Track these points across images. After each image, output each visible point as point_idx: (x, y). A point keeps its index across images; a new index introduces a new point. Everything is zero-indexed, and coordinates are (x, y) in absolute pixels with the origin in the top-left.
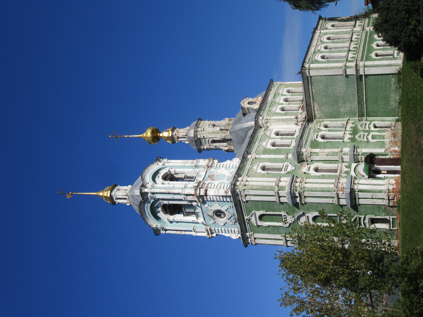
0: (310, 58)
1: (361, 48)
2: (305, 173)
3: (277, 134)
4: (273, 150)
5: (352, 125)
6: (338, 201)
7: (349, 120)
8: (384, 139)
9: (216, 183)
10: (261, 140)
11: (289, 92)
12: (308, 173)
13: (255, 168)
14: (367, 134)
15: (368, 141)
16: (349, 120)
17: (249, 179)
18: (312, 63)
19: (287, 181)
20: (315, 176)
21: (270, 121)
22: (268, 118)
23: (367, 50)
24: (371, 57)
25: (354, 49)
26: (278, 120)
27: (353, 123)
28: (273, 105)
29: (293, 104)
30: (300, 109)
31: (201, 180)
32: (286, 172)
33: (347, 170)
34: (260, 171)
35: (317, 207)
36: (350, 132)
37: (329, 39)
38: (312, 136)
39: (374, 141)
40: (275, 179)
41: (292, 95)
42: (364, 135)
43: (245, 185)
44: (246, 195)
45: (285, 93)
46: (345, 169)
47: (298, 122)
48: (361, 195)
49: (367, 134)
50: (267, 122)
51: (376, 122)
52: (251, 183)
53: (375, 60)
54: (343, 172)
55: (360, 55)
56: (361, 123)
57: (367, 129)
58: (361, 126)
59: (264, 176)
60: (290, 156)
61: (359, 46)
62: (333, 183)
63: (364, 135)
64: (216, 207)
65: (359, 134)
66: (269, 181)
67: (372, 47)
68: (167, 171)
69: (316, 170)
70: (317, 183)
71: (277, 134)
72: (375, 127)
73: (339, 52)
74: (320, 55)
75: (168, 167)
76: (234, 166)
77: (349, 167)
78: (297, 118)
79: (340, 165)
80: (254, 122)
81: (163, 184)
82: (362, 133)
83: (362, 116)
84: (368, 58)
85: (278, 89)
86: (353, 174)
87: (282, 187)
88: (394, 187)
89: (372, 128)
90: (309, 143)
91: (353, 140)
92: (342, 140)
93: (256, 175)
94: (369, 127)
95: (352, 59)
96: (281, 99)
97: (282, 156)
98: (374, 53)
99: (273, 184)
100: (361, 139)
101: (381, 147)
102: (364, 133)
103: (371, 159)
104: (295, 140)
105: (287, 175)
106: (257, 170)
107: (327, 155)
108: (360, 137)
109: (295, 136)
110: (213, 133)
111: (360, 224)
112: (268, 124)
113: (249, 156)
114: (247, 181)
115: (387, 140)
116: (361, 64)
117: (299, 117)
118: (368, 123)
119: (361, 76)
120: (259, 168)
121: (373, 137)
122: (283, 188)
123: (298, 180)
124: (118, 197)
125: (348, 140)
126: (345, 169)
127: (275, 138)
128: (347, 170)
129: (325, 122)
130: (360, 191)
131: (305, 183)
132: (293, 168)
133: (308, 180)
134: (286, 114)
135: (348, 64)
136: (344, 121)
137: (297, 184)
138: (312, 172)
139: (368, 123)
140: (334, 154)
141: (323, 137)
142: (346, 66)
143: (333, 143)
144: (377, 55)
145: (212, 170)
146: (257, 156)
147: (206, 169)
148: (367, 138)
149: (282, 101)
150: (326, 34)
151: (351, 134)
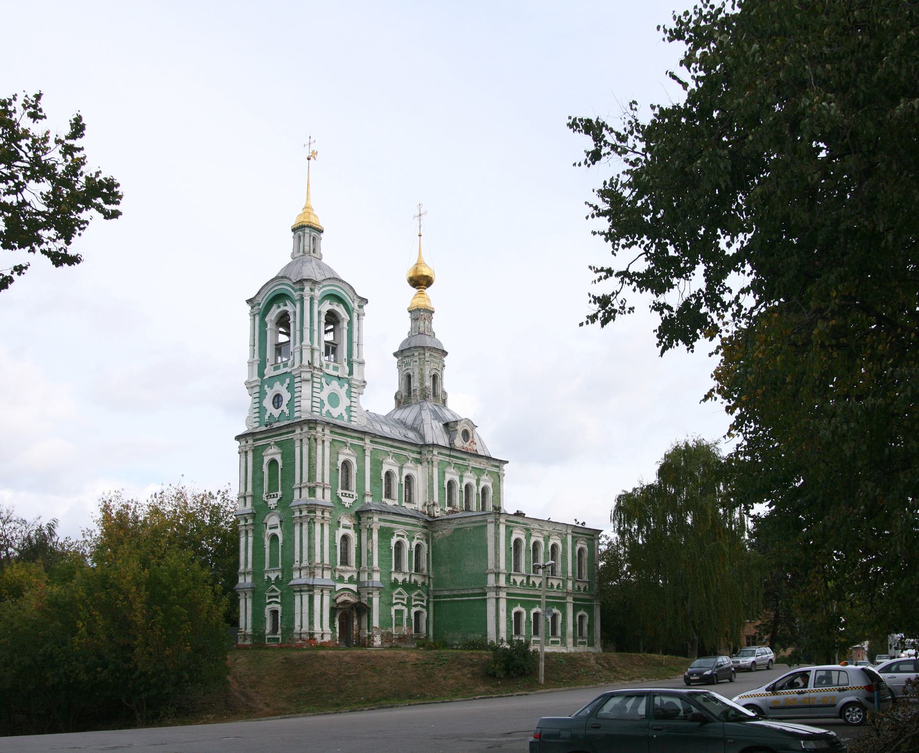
0: (517, 523)
1: (531, 593)
2: (339, 522)
3: (409, 478)
4: (380, 474)
5: (420, 583)
6: (296, 569)
7: (429, 578)
8: (396, 625)
10: (397, 457)
11: (484, 491)
12: (339, 526)
13: (347, 451)
14: (405, 602)
15: (392, 605)
16: (429, 578)
17: (327, 444)
18: (507, 527)
22: (435, 463)
24: (516, 606)
26: (431, 478)
27: (423, 584)
28: (459, 468)
29: (461, 498)
30: (451, 509)
31: (327, 371)
33: (346, 579)
34: (342, 458)
35: (290, 540)
36: (408, 580)
37: (554, 547)
39: (393, 613)
40: (327, 481)
41: (478, 494)
43: (316, 440)
44: (301, 440)
45: (482, 484)
46: (346, 576)
48: (306, 598)
49: (405, 602)
51: (425, 614)
52: (320, 448)
53: (508, 611)
54: (342, 574)
55: (519, 592)
56: (424, 595)
57: (414, 603)
58: (419, 595)
59: (333, 464)
62: (322, 561)
63: (403, 599)
64: (286, 397)
65: (404, 592)
66: (324, 472)
67: (534, 607)
68: (343, 316)
69: (345, 538)
70: (322, 540)
71: (409, 478)
72: (417, 614)
73: (526, 562)
74: (523, 537)
75: (351, 317)
77: (351, 580)
78: (434, 504)
79: (354, 568)
81: (319, 313)
82: (406, 596)
83: (435, 597)
84: (511, 603)
86: (339, 586)
87: (315, 492)
88: (319, 640)
89: (414, 610)
90: (387, 525)
91: (395, 584)
92: (393, 569)
93: (335, 454)
94: (416, 606)
96: (470, 478)
98: (523, 610)
99: (319, 479)
100: (395, 596)
103: (363, 609)
106: (343, 454)
107: (368, 551)
108: (400, 593)
109: (404, 504)
111: (270, 597)
112: (425, 464)
113: (367, 441)
114: (323, 441)
115: (394, 630)
116: (503, 594)
117: (435, 508)
118: (425, 604)
119: (485, 594)
120: (347, 457)
121: (398, 612)
122: (312, 491)
123: (327, 515)
125: (393, 579)
126: (346, 576)
128: (346, 579)
129: (426, 545)
130: (311, 599)
131: (322, 525)
132: (347, 505)
134: (441, 488)
135: (502, 578)
136: (428, 570)
137: (319, 513)
138: (341, 532)
139: (425, 604)
140: (370, 559)
141: (399, 544)
142: (499, 573)
144: (518, 614)
145: (346, 386)
146: (368, 453)
149: (466, 481)
150: (564, 542)
151: (404, 581)
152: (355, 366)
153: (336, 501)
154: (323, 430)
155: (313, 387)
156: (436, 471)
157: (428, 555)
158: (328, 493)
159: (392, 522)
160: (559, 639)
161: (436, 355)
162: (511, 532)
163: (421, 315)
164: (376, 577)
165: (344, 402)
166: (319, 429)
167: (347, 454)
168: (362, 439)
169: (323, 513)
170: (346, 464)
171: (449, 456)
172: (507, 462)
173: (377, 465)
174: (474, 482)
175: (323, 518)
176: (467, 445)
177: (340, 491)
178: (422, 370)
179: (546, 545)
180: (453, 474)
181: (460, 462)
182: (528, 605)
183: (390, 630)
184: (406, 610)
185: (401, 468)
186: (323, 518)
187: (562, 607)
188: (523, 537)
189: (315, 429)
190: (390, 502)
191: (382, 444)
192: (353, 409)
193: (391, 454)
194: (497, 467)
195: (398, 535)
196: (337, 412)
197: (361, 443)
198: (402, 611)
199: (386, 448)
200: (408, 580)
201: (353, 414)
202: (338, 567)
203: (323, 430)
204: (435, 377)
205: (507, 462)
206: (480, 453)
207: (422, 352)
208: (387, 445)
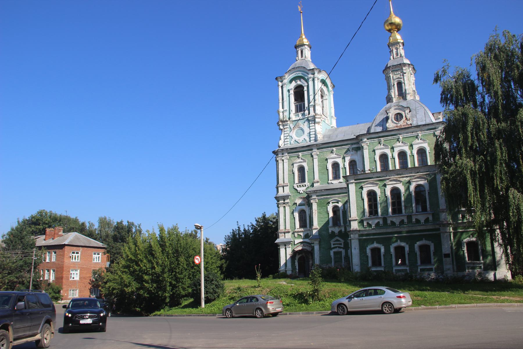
8: (335, 262)
14: (342, 246)
15: (332, 249)
24: (373, 243)
25: (389, 222)
32: (296, 188)
36: (343, 230)
42: (341, 244)
49: (342, 246)
54: (299, 233)
63: (341, 244)
75: (308, 83)
91: (333, 234)
97: (317, 178)
99: (281, 182)
100: (332, 243)
101: (321, 260)
102: (343, 244)
106: (296, 163)
108: (337, 240)
114: (283, 160)
124: (304, 51)
125: (330, 231)
133: (287, 208)
148: (334, 248)
151: (340, 232)
152: (312, 109)
161: (397, 69)
162: (362, 188)
167: (300, 162)
177: (295, 186)
183: (329, 265)
184: (343, 251)
190: (336, 182)
194: (435, 128)
198: (341, 252)
200: (343, 230)
206: (420, 124)
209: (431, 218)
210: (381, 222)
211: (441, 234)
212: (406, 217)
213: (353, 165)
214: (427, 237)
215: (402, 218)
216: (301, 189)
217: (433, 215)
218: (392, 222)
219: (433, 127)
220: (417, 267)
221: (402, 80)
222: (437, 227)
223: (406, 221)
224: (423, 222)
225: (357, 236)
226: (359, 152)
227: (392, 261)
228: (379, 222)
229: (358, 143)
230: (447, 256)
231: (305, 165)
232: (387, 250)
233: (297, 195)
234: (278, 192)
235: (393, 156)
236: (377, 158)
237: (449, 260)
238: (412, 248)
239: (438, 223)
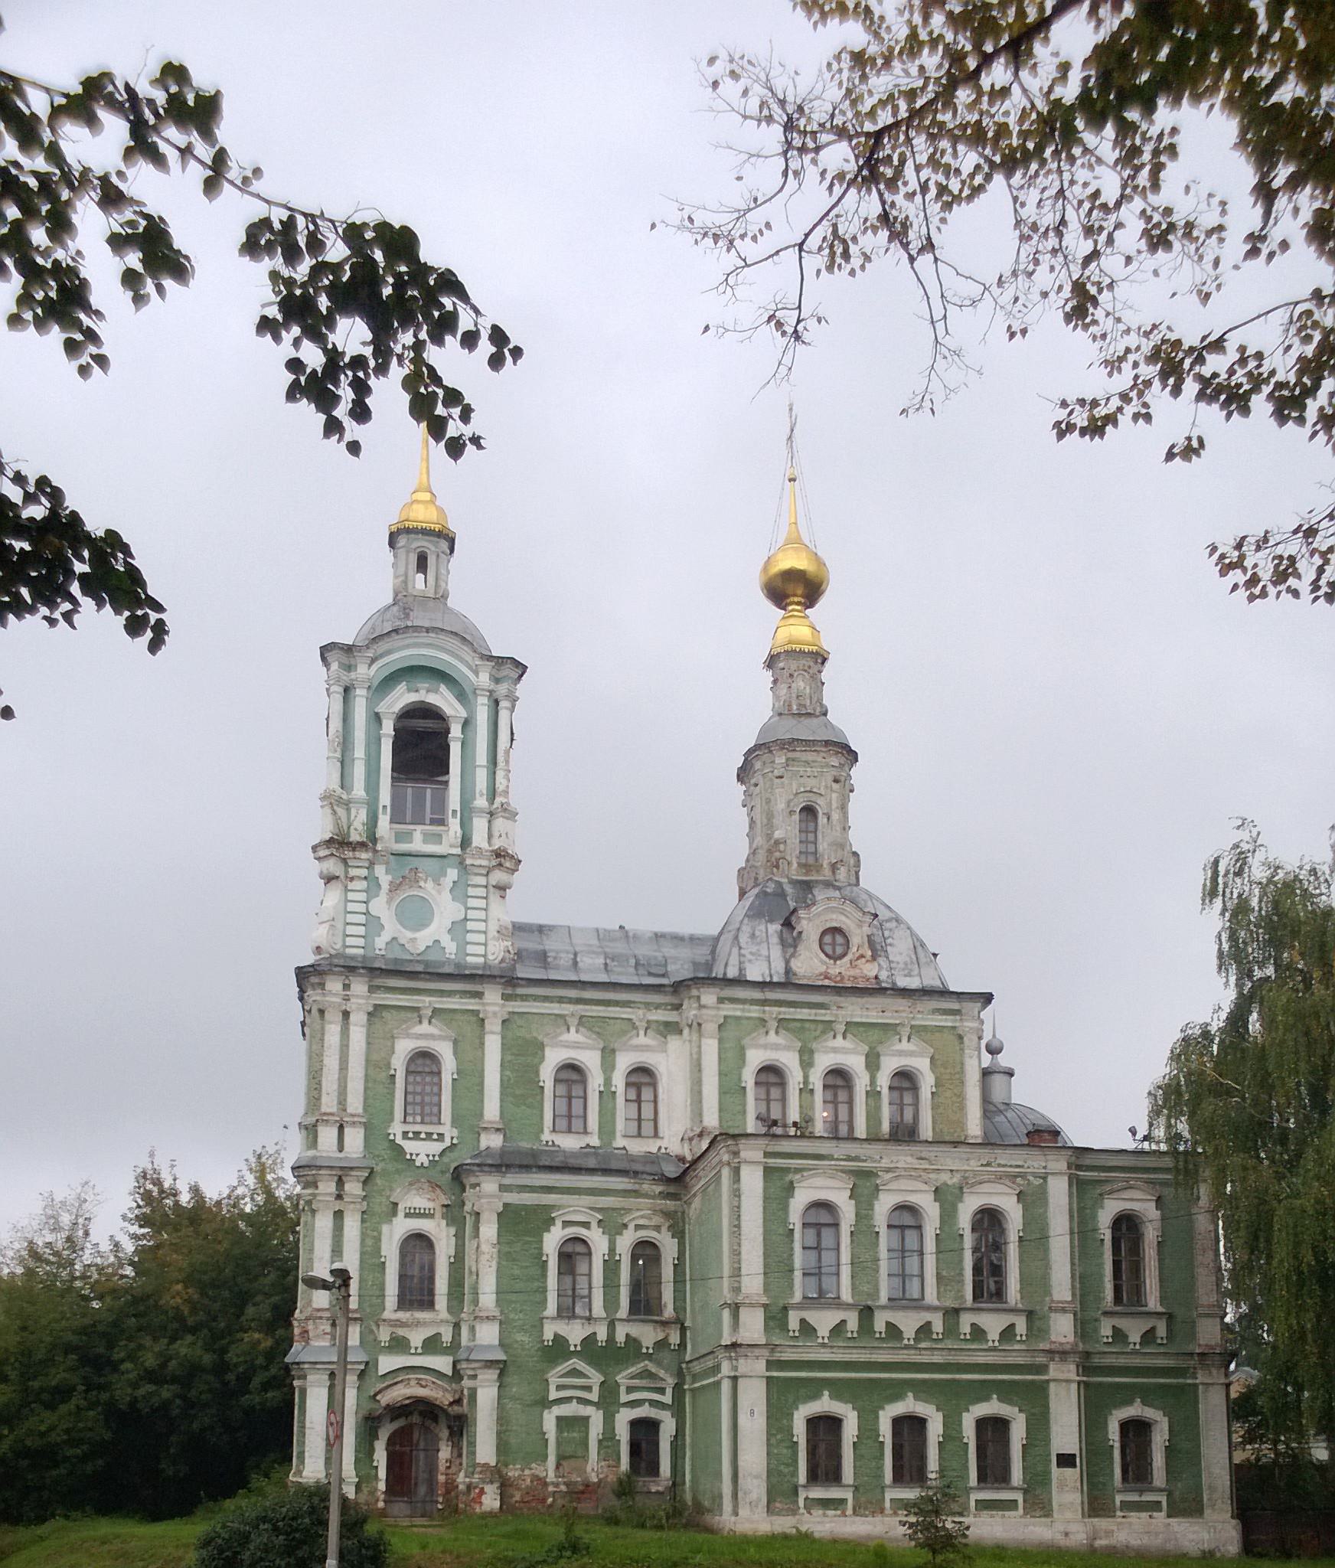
9: (380, 906)
12: (394, 1213)
13: (425, 1028)
17: (358, 1019)
18: (768, 1171)
19: (341, 1149)
20: (378, 1239)
21: (695, 1037)
22: (710, 1027)
23: (871, 1380)
24: (816, 1396)
25: (879, 1326)
26: (697, 1067)
32: (399, 1140)
34: (404, 1048)
38: (577, 1208)
40: (355, 1104)
43: (322, 1012)
47: (691, 1139)
50: (690, 1026)
55: (825, 1355)
60: (493, 1141)
61: (907, 1347)
67: (898, 1397)
74: (840, 1197)
76: (470, 949)
80: (732, 973)
85: (918, 1031)
87: (316, 1137)
95: (793, 1323)
97: (492, 1109)
99: (329, 1103)
104: (595, 1141)
105: (386, 1144)
106: (408, 1036)
109: (620, 1142)
110: (770, 816)
113: (493, 996)
114: (346, 1014)
123: (353, 1188)
127: (608, 1066)
131: (339, 1215)
137: (327, 1187)
138: (400, 1227)
143: (536, 1284)
145: (452, 874)
146: (493, 1026)
147: (458, 851)
149: (824, 1061)
152: (479, 825)
153: (386, 1154)
154: (346, 987)
155: (346, 890)
156: (710, 1048)
157: (678, 1267)
158: (355, 1140)
159: (549, 1190)
160: (1019, 1497)
161: (810, 757)
162: (790, 1189)
163: (798, 666)
164: (488, 1334)
165: (446, 909)
166: (334, 985)
168: (479, 995)
169: (340, 1183)
170: (424, 1061)
171: (764, 1002)
172: (987, 998)
173: (522, 1056)
174: (856, 1063)
175: (339, 1197)
176: (840, 968)
177: (396, 1129)
178: (768, 801)
179: (948, 1215)
180: (776, 1047)
181: (804, 1014)
182: (867, 1394)
185: (608, 1056)
186: (339, 1197)
187: (1034, 1398)
188: (840, 1197)
189: (322, 985)
191: (546, 999)
192: (470, 925)
193: (573, 1022)
194: (957, 1012)
195: (566, 1224)
196: (433, 936)
197: (471, 1004)
199: (555, 1008)
201: (470, 937)
202: (387, 1315)
203: (346, 987)
204: (809, 811)
205: (987, 998)
206: (902, 982)
207: (767, 757)
208: (561, 1000)
209: (1021, 1327)
210: (853, 1324)
211: (1052, 1385)
212: (940, 1315)
213: (638, 1087)
214: (1007, 1392)
215: (927, 1316)
216: (422, 1151)
217: (1030, 1315)
218: (888, 1324)
219: (956, 1006)
220: (968, 1490)
221: (821, 801)
222: (1041, 1359)
223: (938, 1326)
224: (997, 1338)
225: (761, 1366)
226: (674, 1043)
227: (881, 1468)
228: (843, 1322)
229: (678, 1007)
230: (1066, 1460)
231: (445, 1051)
232: (869, 1429)
233: (398, 1172)
234: (312, 1140)
235: (806, 1082)
236: (749, 1077)
237: (1071, 1474)
238: (952, 1426)
239: (1042, 1346)
